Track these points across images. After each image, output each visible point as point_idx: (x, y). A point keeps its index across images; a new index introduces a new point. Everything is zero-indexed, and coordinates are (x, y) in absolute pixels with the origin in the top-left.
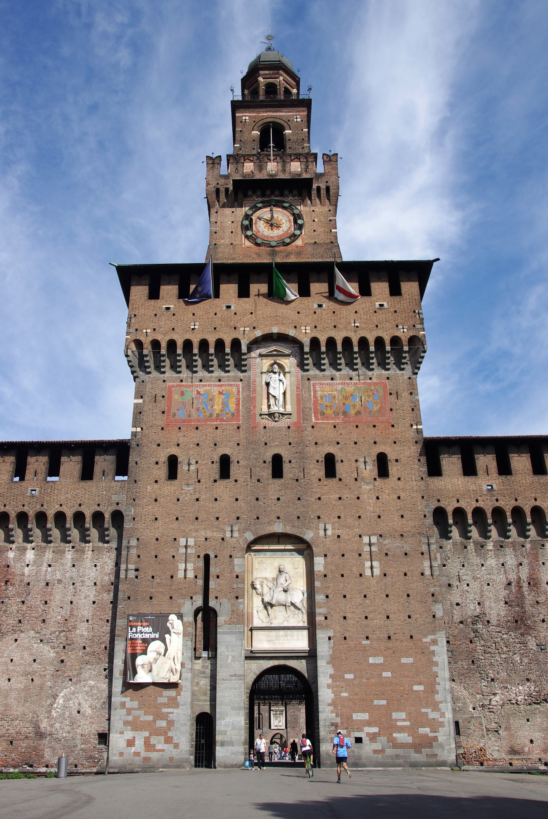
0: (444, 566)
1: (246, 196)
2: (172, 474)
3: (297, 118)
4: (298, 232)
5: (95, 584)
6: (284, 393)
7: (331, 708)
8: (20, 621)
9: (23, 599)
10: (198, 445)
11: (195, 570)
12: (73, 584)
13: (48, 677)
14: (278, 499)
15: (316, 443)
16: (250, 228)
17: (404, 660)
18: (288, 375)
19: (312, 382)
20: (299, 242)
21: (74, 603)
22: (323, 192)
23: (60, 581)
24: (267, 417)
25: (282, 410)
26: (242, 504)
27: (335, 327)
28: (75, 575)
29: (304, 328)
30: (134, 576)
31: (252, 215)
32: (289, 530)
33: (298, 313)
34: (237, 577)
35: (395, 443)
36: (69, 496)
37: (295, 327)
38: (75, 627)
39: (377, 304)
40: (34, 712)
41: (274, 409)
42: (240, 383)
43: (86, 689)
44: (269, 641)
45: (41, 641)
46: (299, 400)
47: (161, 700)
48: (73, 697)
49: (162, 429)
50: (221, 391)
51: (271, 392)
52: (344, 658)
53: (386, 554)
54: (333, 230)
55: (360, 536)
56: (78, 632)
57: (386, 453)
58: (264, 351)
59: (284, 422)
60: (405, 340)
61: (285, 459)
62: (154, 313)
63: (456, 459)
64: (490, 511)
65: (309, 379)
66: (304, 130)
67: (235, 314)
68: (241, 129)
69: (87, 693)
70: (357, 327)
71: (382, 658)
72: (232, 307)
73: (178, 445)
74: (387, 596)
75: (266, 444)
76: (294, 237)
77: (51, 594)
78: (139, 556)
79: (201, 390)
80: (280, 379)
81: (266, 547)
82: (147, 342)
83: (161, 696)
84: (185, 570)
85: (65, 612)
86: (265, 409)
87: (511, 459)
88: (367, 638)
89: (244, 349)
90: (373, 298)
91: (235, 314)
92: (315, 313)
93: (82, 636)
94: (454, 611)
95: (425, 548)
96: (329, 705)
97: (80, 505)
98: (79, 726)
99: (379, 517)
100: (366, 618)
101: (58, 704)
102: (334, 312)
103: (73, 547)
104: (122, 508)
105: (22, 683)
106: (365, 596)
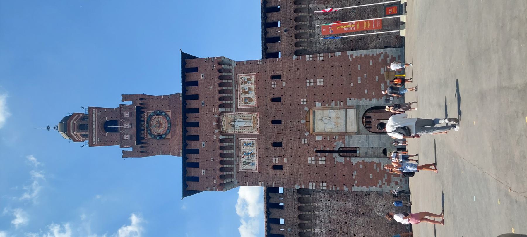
0: (319, 51)
1: (144, 138)
3: (99, 114)
4: (164, 114)
5: (329, 201)
6: (244, 119)
7: (380, 99)
8: (347, 234)
9: (337, 233)
10: (267, 157)
11: (322, 157)
12: (329, 210)
13: (370, 220)
14: (291, 121)
15: (266, 106)
16: (161, 136)
17: (359, 69)
18: (236, 118)
19: (239, 107)
20: (169, 113)
21: (338, 209)
22: (142, 101)
23: (328, 216)
24: (254, 127)
25: (252, 121)
26: (293, 137)
27: (213, 97)
28: (325, 210)
29: (214, 111)
30: (325, 184)
31: (154, 135)
32: (304, 117)
33: (206, 113)
34: (325, 139)
35: (266, 72)
36: (291, 214)
37: (213, 115)
38: (348, 209)
39: (202, 78)
40: (385, 225)
41: (251, 124)
42: (239, 139)
43: (374, 203)
44: (352, 125)
45: (355, 224)
47: (378, 171)
48: (378, 208)
49: (260, 173)
50: (243, 147)
51: (243, 126)
52: (359, 94)
53: (314, 76)
54: (162, 97)
55: (306, 87)
56: (350, 207)
57: (270, 75)
58: (224, 129)
62: (206, 179)
63: (273, 45)
64: (296, 31)
65: (237, 109)
66: (106, 111)
67: (207, 141)
68: (105, 142)
69: (376, 202)
70: (213, 87)
71: (359, 78)
72: (204, 143)
73: (267, 165)
74: (332, 76)
75: (266, 127)
76: (166, 115)
77: (334, 220)
78: (317, 181)
80: (237, 121)
81: (311, 126)
83: (376, 170)
84: (322, 161)
85: (342, 213)
87: (273, 21)
88: (350, 84)
90: (199, 80)
91: (207, 141)
92: (206, 106)
93: (352, 206)
94: (339, 47)
96: (378, 100)
97: (295, 208)
98: (390, 205)
99: (298, 79)
100: (341, 84)
101: (381, 215)
102: (206, 97)
103: (313, 211)
105: (373, 231)
106: (332, 85)
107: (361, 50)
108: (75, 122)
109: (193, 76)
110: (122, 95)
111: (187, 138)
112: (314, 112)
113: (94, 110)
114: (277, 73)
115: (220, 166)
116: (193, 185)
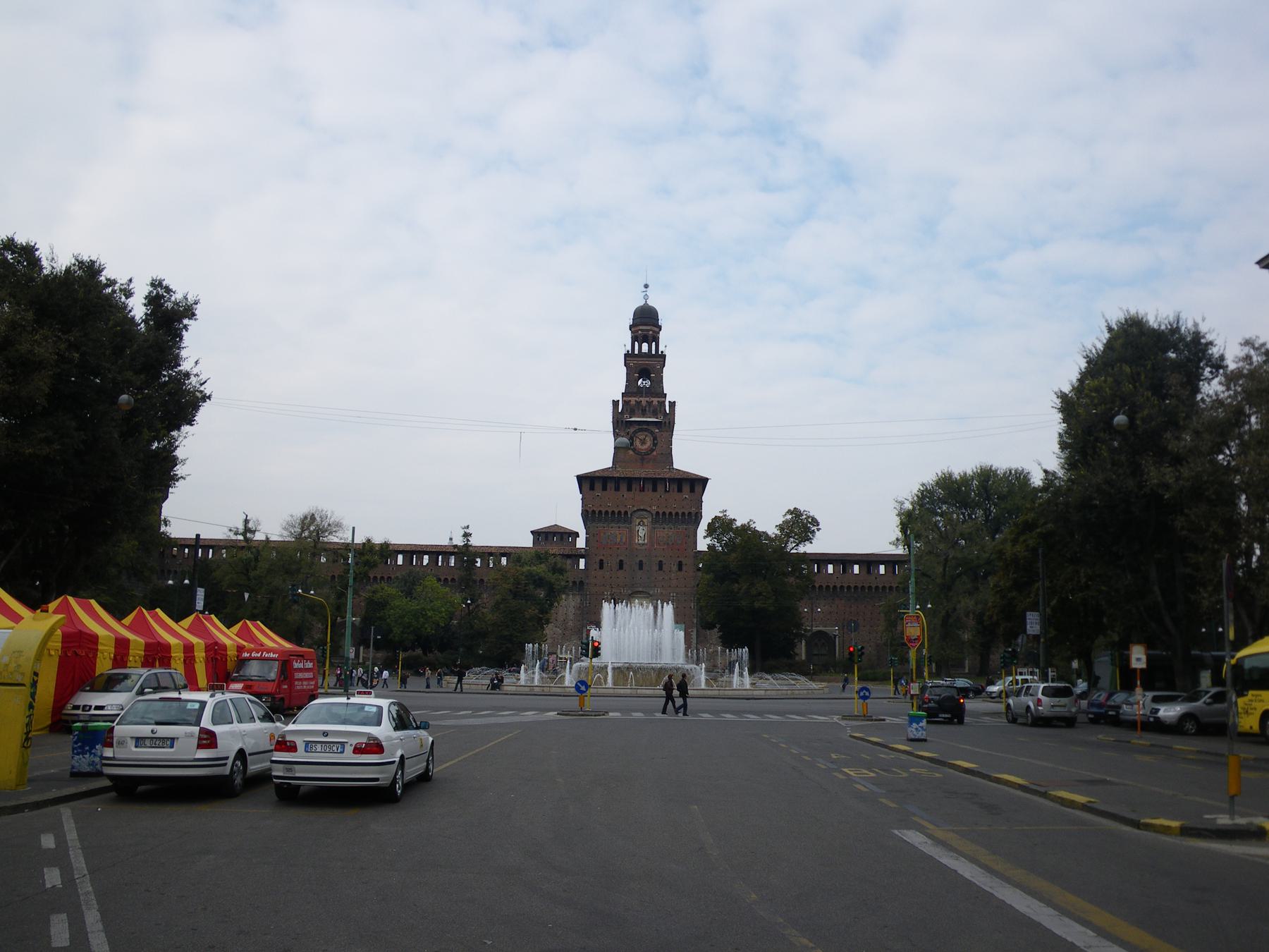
2: (601, 567)
20: (655, 453)
22: (667, 424)
32: (645, 590)
38: (567, 623)
41: (640, 542)
46: (650, 538)
59: (643, 548)
60: (693, 514)
61: (644, 562)
76: (652, 450)
79: (612, 532)
82: (590, 511)
86: (637, 541)
89: (629, 516)
95: (692, 599)
104: (583, 580)
107: (697, 638)
108: (651, 332)
109: (686, 488)
110: (675, 402)
111: (630, 482)
112: (648, 598)
113: (662, 360)
114: (684, 568)
115: (603, 511)
116: (586, 486)
